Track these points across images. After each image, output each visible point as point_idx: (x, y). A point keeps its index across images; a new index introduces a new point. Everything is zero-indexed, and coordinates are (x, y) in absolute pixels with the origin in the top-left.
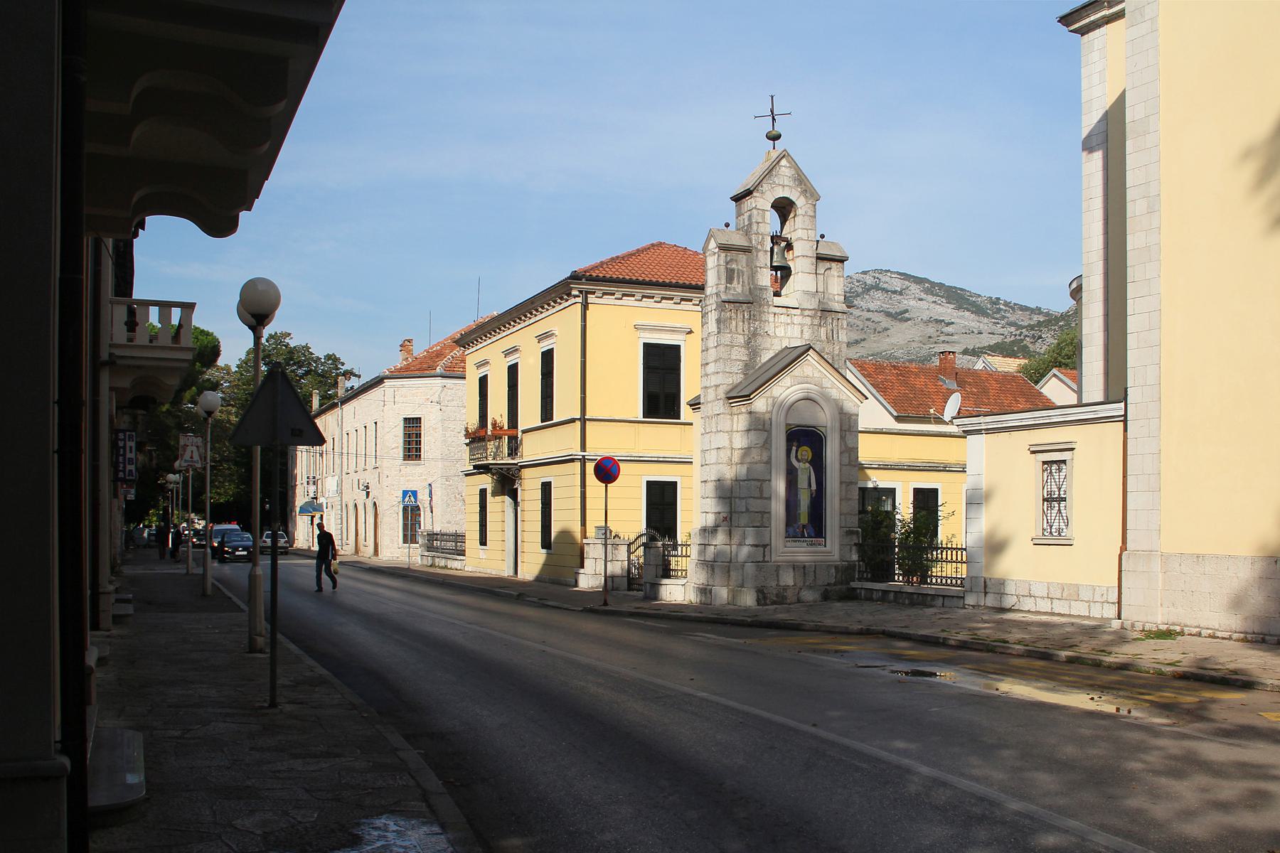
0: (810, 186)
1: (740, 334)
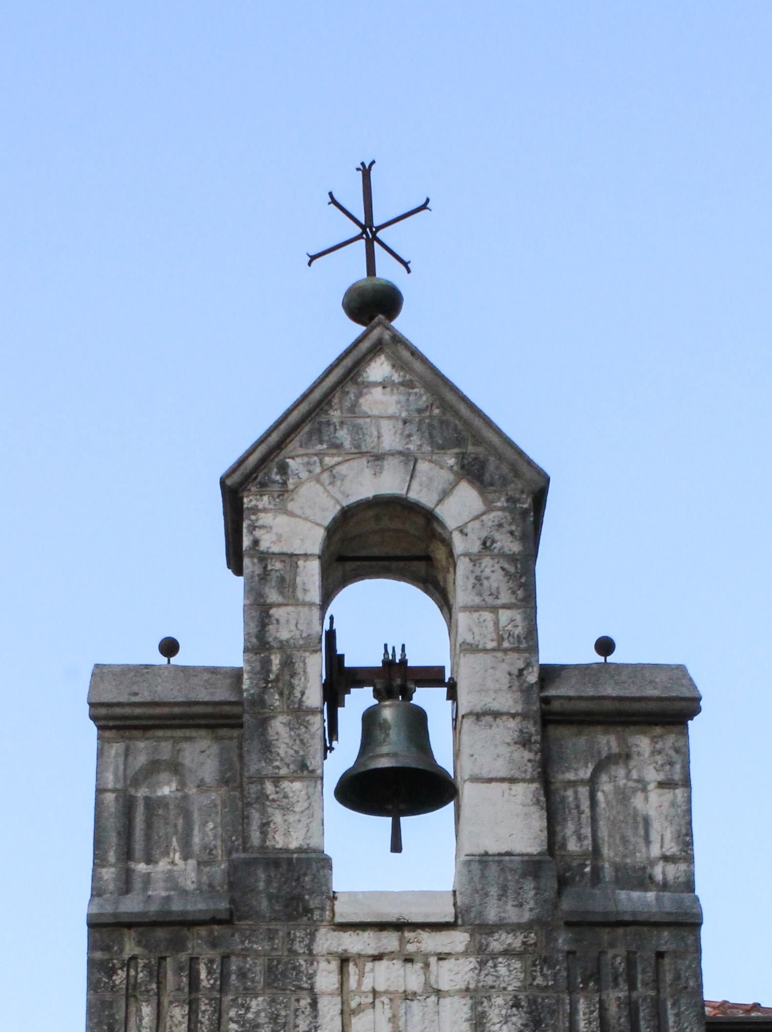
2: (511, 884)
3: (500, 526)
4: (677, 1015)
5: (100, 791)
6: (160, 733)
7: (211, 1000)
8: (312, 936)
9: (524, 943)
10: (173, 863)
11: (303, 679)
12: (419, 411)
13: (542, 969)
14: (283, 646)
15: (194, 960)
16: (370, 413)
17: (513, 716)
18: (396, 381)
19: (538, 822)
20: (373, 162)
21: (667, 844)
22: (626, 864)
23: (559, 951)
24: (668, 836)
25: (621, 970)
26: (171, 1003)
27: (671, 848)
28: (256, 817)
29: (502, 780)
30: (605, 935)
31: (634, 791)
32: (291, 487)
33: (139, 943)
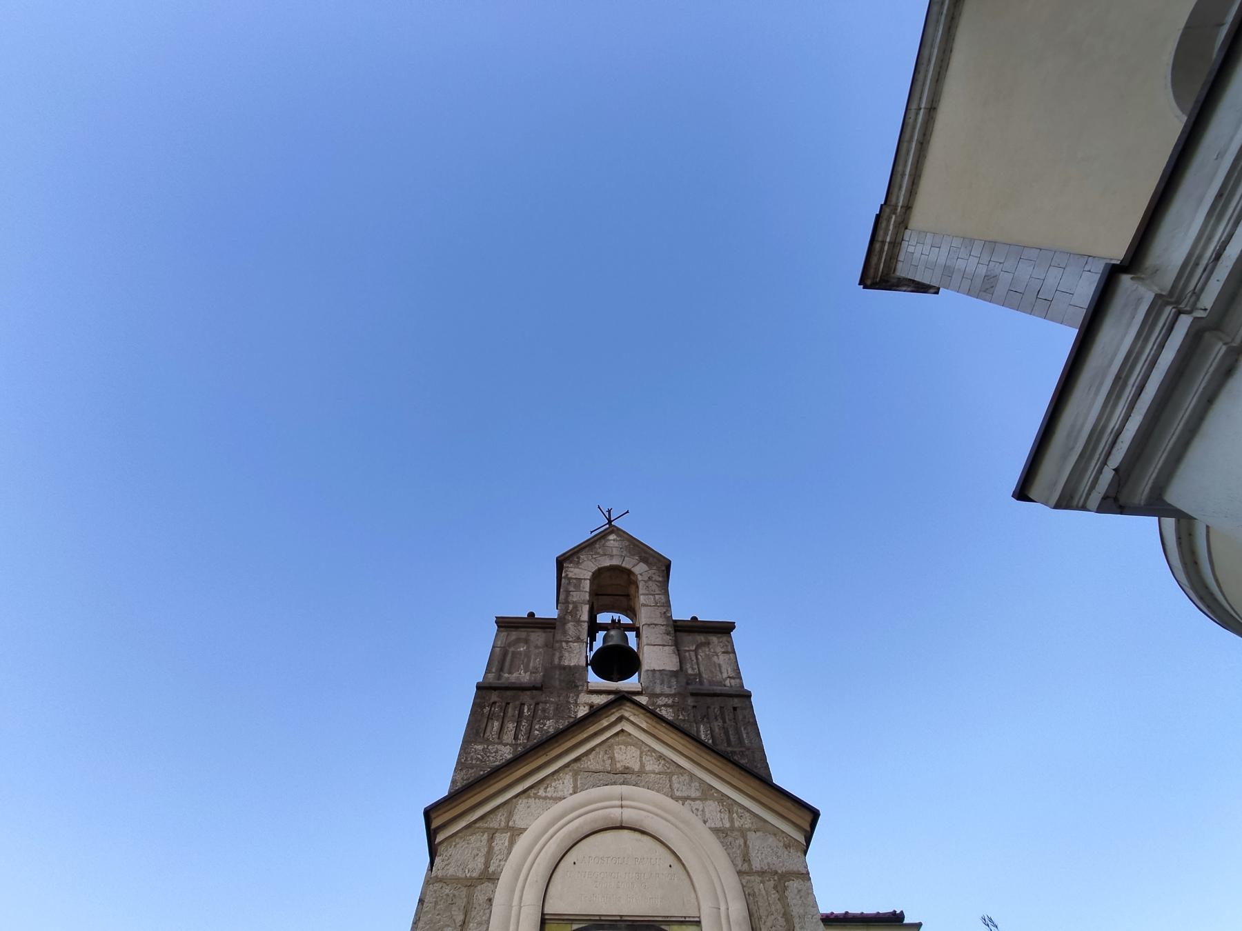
1: (505, 745)
4: (747, 733)
5: (494, 647)
6: (522, 629)
7: (527, 720)
10: (520, 674)
14: (574, 603)
15: (523, 704)
17: (663, 625)
19: (675, 660)
21: (729, 673)
22: (713, 681)
24: (729, 669)
27: (732, 674)
28: (557, 654)
30: (709, 700)
31: (713, 656)
33: (498, 697)
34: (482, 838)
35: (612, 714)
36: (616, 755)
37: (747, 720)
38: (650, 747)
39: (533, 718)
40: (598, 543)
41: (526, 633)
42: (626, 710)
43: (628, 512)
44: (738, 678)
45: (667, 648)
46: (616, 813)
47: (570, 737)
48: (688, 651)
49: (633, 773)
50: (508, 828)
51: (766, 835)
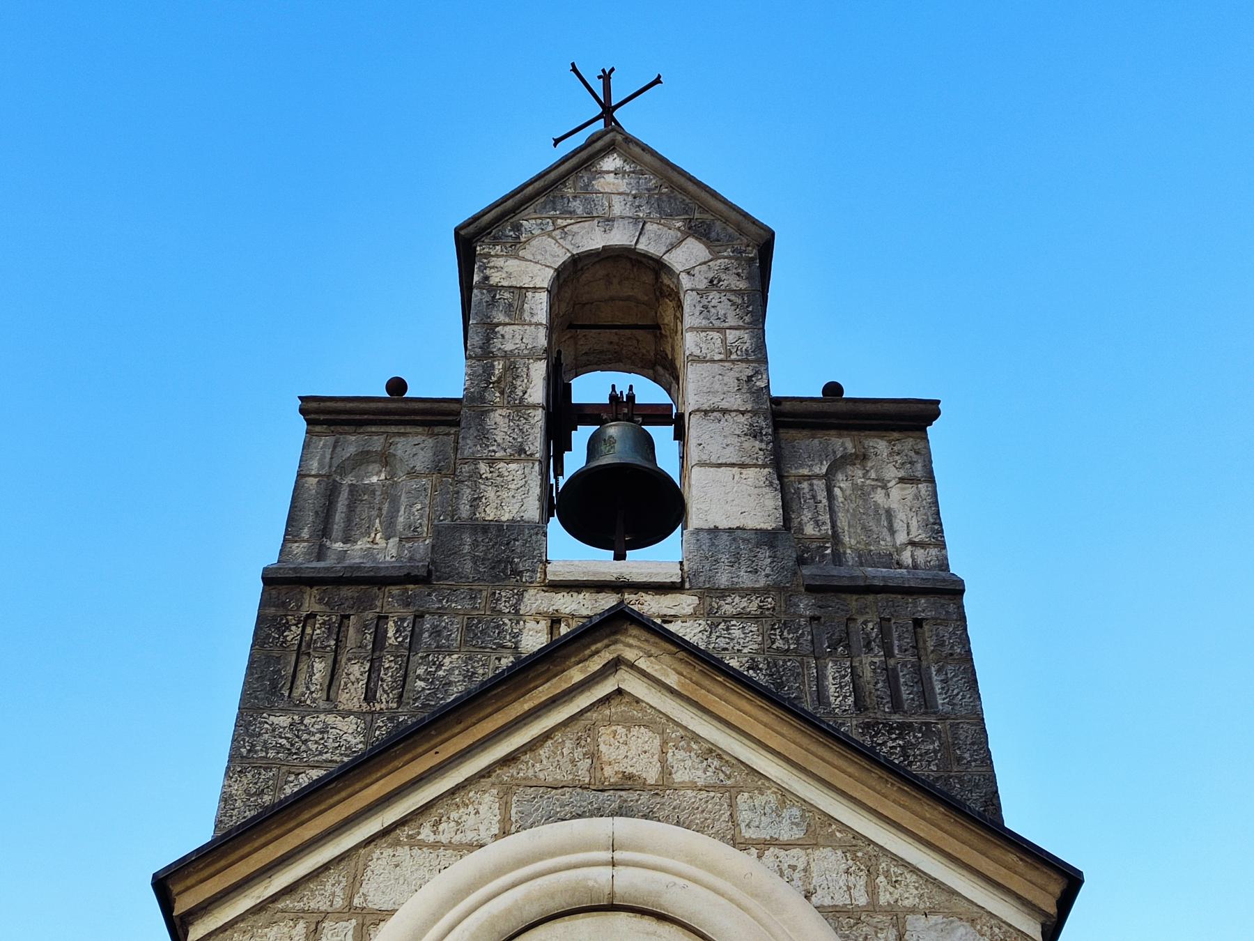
0: (721, 206)
1: (345, 714)
2: (745, 554)
3: (727, 269)
4: (945, 681)
8: (520, 596)
9: (760, 607)
11: (526, 381)
12: (649, 190)
13: (782, 632)
14: (506, 355)
15: (383, 618)
16: (602, 190)
17: (743, 413)
18: (627, 170)
19: (772, 501)
20: (613, 70)
23: (801, 616)
24: (914, 523)
25: (874, 635)
26: (349, 660)
27: (919, 534)
28: (467, 493)
29: (733, 465)
30: (853, 602)
31: (874, 488)
32: (523, 240)
33: (320, 601)
34: (294, 932)
35: (592, 655)
36: (603, 748)
37: (947, 650)
38: (685, 728)
39: (410, 650)
40: (570, 183)
41: (382, 439)
42: (630, 646)
43: (658, 81)
44: (936, 546)
45: (751, 472)
46: (599, 879)
47: (489, 710)
48: (809, 478)
49: (644, 787)
50: (350, 910)
51: (952, 922)
